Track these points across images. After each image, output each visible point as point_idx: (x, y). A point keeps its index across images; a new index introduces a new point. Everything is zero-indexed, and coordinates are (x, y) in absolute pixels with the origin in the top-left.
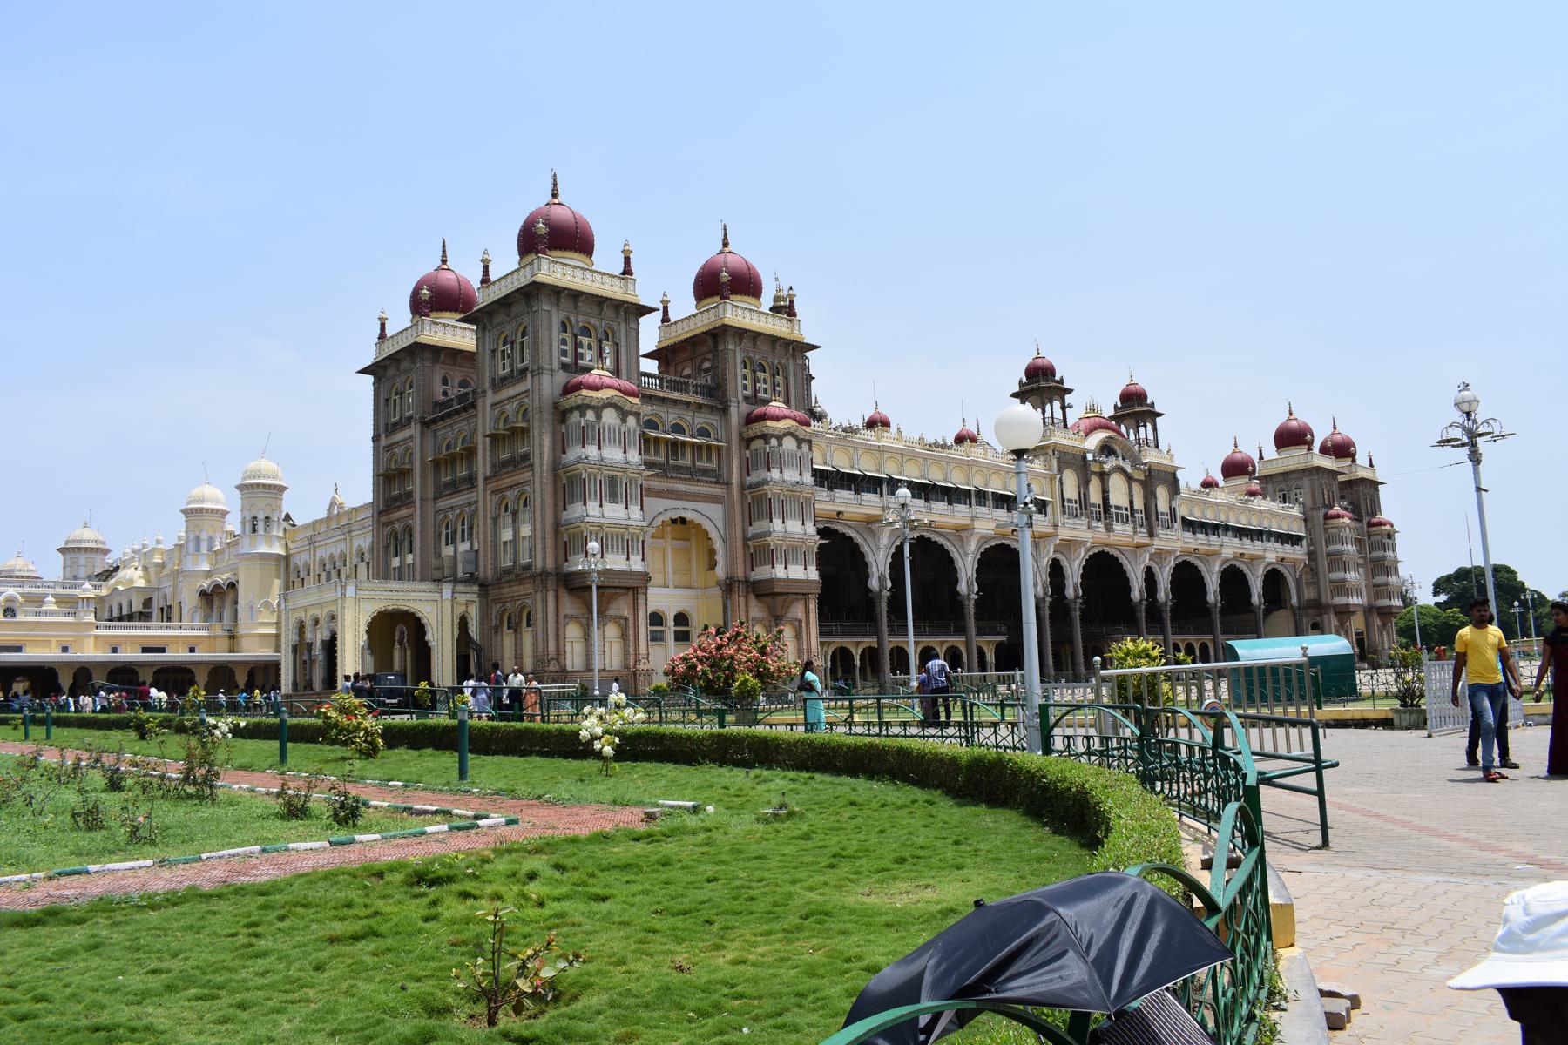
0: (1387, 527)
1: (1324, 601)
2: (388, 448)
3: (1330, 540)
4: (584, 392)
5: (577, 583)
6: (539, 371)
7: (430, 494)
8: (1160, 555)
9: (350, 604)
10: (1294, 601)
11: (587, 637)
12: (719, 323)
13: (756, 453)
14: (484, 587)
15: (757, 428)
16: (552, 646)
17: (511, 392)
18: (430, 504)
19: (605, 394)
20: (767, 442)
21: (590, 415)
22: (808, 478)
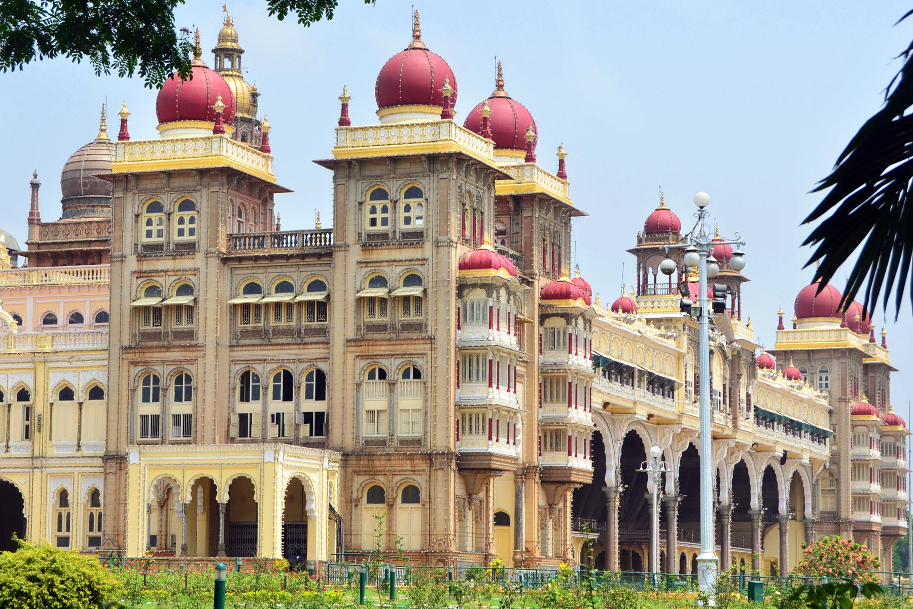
0: (900, 428)
1: (843, 515)
2: (140, 274)
3: (856, 441)
4: (492, 272)
5: (476, 464)
6: (450, 244)
7: (226, 340)
8: (739, 446)
9: (279, 468)
10: (808, 511)
11: (461, 518)
12: (523, 190)
13: (553, 332)
14: (346, 456)
15: (561, 304)
16: (452, 529)
17: (396, 254)
18: (225, 352)
19: (503, 273)
20: (569, 323)
21: (495, 295)
22: (590, 363)
